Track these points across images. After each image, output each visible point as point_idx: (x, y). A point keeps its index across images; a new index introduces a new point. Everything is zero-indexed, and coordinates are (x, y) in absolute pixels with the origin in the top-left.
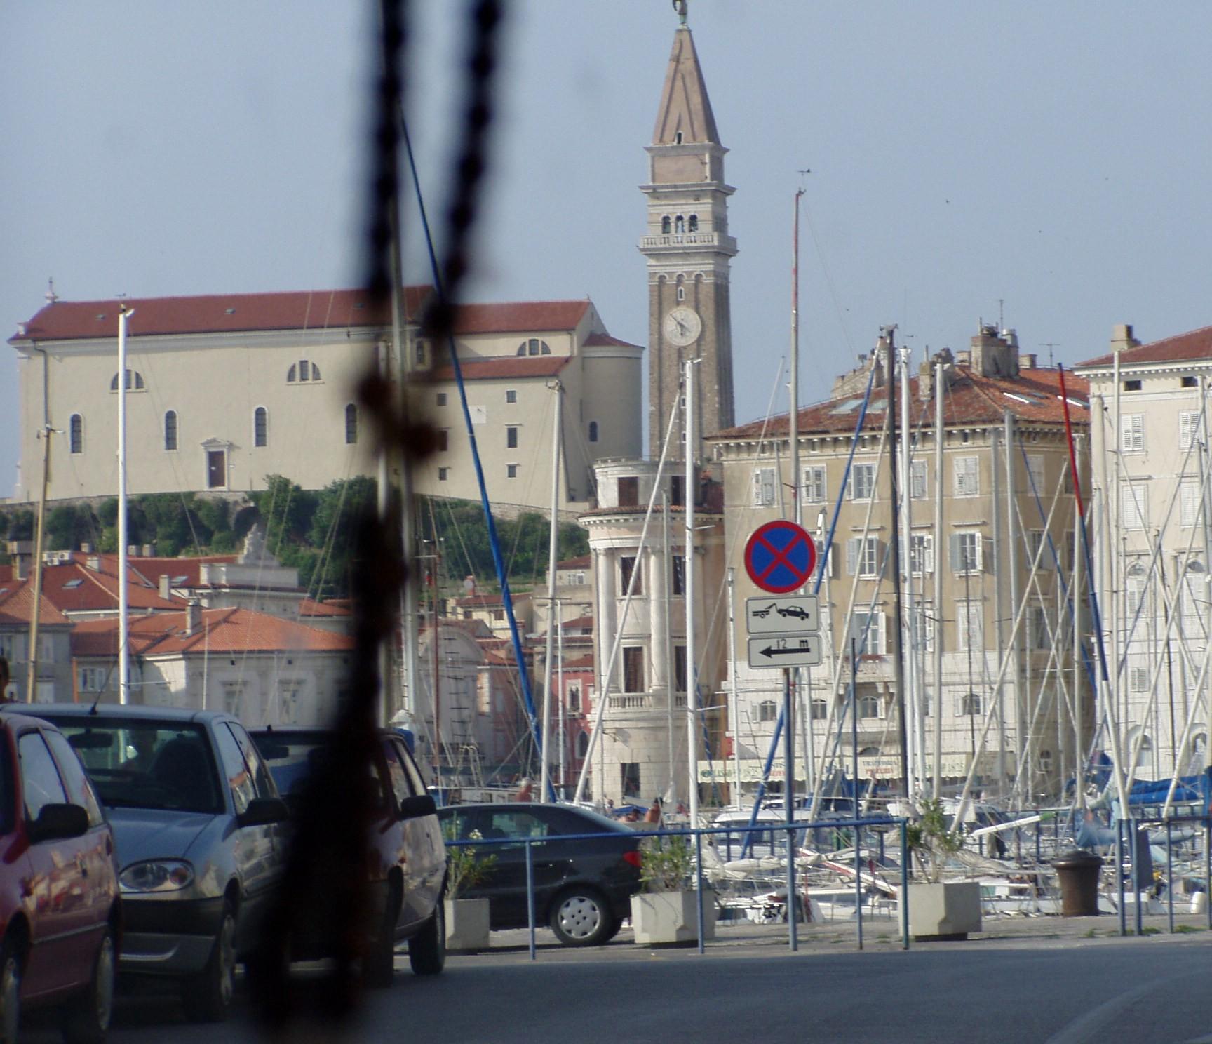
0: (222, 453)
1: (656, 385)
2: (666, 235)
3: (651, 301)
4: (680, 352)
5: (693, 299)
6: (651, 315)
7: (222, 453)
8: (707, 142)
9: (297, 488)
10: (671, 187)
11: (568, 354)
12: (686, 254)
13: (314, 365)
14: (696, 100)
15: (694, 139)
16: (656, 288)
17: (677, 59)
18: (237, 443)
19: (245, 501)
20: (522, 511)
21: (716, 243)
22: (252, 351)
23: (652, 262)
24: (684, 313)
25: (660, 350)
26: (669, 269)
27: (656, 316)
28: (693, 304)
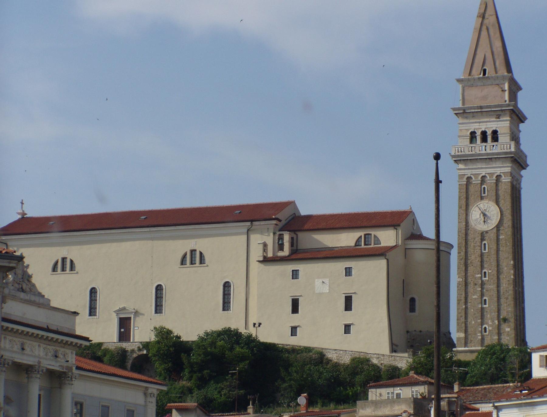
0: (130, 318)
1: (463, 262)
2: (472, 145)
3: (460, 197)
4: (483, 235)
5: (494, 193)
6: (460, 207)
7: (130, 318)
8: (506, 74)
9: (178, 337)
10: (478, 108)
11: (394, 244)
12: (490, 159)
13: (201, 253)
14: (498, 44)
15: (496, 73)
16: (465, 186)
17: (483, 16)
18: (142, 311)
19: (140, 349)
20: (354, 356)
21: (513, 149)
22: (156, 242)
23: (461, 166)
24: (486, 205)
25: (466, 234)
26: (475, 172)
27: (464, 208)
28: (494, 198)
